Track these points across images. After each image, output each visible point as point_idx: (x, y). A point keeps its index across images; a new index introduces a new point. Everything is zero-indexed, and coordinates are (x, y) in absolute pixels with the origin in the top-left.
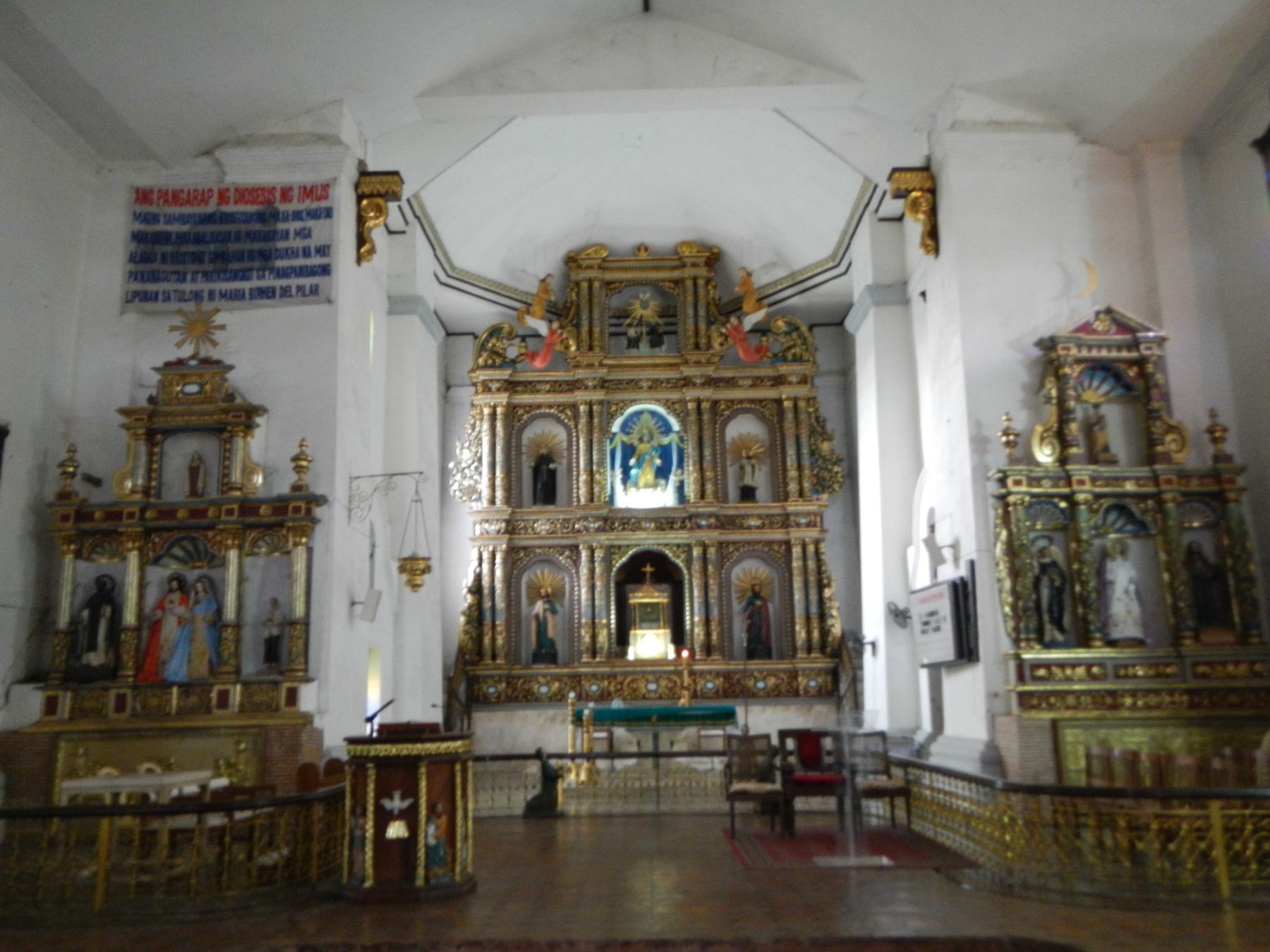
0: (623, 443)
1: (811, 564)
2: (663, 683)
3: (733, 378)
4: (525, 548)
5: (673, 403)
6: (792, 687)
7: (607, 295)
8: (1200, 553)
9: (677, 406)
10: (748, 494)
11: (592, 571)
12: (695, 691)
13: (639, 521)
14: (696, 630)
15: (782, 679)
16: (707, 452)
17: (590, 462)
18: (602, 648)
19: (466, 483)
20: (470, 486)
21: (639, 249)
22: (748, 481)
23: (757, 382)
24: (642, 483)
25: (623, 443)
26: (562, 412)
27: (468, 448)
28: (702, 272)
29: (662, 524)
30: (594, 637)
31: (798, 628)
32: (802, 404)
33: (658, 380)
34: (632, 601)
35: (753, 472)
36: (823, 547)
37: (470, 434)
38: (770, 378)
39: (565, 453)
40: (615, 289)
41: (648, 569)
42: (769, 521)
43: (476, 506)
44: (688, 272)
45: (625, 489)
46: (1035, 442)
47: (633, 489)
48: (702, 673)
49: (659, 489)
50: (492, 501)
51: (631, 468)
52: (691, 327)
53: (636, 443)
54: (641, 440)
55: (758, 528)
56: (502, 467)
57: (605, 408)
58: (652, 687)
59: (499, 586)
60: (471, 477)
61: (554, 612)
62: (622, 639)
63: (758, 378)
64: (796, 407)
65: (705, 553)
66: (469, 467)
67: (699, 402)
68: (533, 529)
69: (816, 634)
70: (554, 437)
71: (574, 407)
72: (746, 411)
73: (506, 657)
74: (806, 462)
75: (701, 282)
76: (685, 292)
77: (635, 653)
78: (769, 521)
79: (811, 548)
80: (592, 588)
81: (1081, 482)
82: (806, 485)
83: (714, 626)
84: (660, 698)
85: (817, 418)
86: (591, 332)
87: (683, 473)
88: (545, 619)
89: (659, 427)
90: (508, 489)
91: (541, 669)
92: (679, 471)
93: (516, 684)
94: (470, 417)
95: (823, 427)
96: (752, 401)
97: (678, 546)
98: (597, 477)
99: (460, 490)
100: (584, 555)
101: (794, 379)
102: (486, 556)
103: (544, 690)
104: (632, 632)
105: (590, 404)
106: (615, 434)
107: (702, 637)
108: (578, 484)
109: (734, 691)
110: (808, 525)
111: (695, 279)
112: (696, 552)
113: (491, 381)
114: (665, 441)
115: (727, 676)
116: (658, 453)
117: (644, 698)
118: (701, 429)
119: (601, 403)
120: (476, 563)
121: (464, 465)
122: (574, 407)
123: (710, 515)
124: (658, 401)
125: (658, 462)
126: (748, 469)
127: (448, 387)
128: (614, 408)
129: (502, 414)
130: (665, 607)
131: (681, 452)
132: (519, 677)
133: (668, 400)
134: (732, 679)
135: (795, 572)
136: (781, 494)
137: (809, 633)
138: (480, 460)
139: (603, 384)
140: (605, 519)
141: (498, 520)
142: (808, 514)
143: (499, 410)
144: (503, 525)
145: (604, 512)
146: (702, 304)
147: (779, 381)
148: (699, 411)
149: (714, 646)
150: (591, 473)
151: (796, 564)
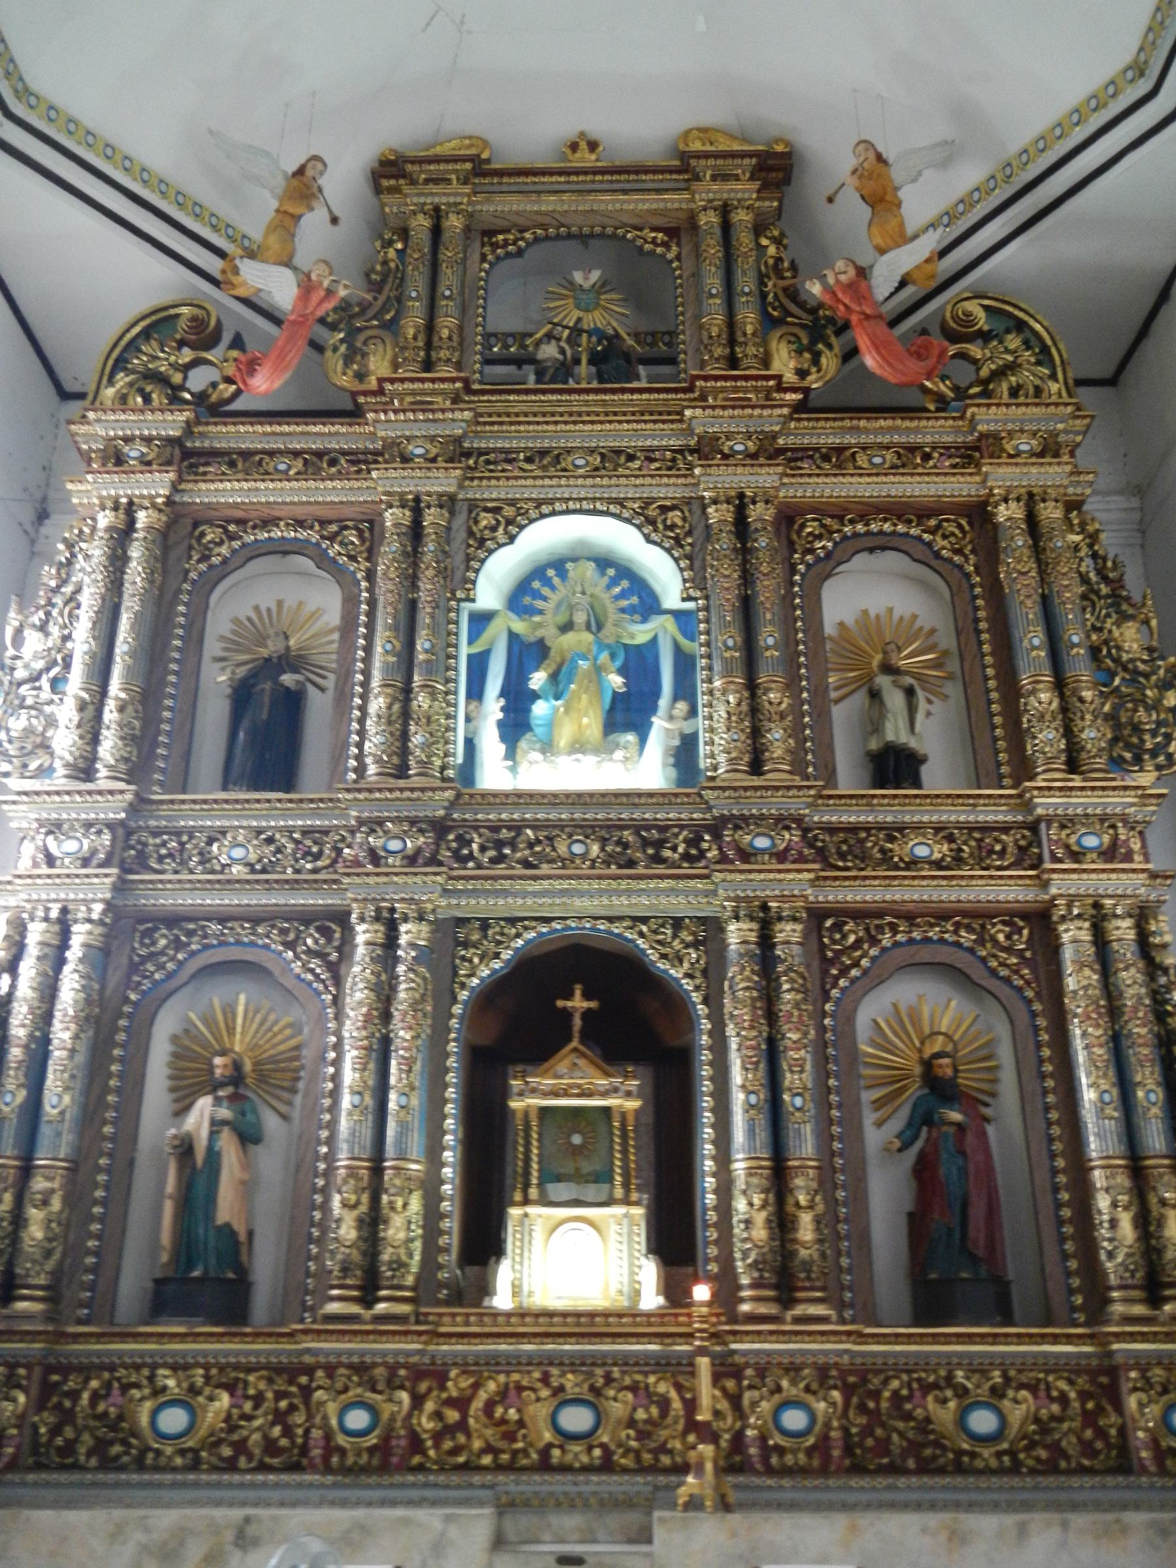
0: (513, 636)
1: (1131, 980)
2: (618, 1406)
4: (173, 920)
5: (664, 509)
6: (1101, 1433)
7: (483, 258)
9: (675, 517)
12: (738, 1438)
13: (550, 831)
14: (740, 1205)
15: (1063, 1399)
16: (768, 637)
18: (399, 1265)
21: (574, 147)
22: (895, 731)
24: (564, 738)
25: (513, 636)
26: (332, 538)
28: (744, 190)
29: (626, 846)
31: (1103, 1202)
32: (1051, 513)
33: (618, 452)
34: (515, 1104)
35: (912, 710)
36: (1163, 929)
38: (948, 450)
40: (506, 243)
41: (578, 1003)
44: (709, 191)
45: (511, 754)
47: (536, 756)
49: (619, 754)
50: (84, 770)
51: (535, 696)
52: (715, 320)
53: (549, 633)
54: (567, 627)
56: (129, 671)
57: (460, 520)
58: (577, 1419)
59: (62, 1034)
61: (249, 1137)
63: (912, 449)
64: (1032, 522)
65: (766, 941)
66: (38, 678)
67: (741, 504)
68: (205, 858)
71: (370, 528)
72: (879, 545)
73: (54, 1294)
74: (1082, 672)
75: (741, 217)
76: (697, 253)
77: (516, 1290)
79: (1123, 930)
80: (381, 1050)
83: (802, 1190)
84: (607, 1466)
87: (693, 712)
88: (213, 1156)
89: (623, 595)
92: (682, 707)
93: (75, 1395)
94: (61, 546)
96: (897, 510)
97: (677, 923)
98: (421, 701)
100: (364, 934)
101: (1025, 445)
102: (36, 933)
104: (514, 1212)
107: (760, 1233)
108: (361, 721)
109: (883, 1447)
110: (1110, 853)
111: (725, 210)
112: (738, 934)
113: (127, 440)
114: (640, 633)
116: (619, 663)
117: (545, 1465)
118: (747, 578)
119: (449, 502)
123: (782, 822)
124: (615, 508)
125: (616, 681)
126: (895, 700)
127: (42, 516)
128: (486, 520)
129: (149, 528)
130: (631, 1119)
131: (684, 664)
132: (86, 1371)
133: (647, 502)
134: (876, 1395)
135: (1076, 1006)
140: (440, 828)
141: (88, 825)
142: (1106, 820)
144: (106, 838)
145: (436, 805)
148: (741, 526)
149: (807, 1265)
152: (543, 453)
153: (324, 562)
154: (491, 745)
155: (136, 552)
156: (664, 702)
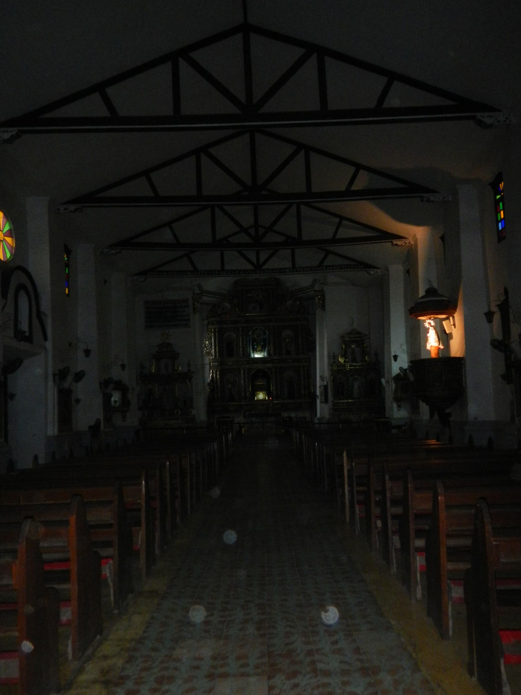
10: (288, 353)
11: (244, 375)
17: (243, 344)
19: (208, 351)
20: (209, 352)
30: (245, 394)
37: (208, 336)
43: (211, 358)
46: (340, 358)
50: (215, 356)
60: (209, 349)
62: (254, 394)
69: (307, 392)
81: (348, 366)
98: (245, 349)
103: (232, 409)
106: (250, 335)
138: (211, 344)
143: (216, 329)
150: (243, 348)
154: (251, 351)
156: (267, 345)
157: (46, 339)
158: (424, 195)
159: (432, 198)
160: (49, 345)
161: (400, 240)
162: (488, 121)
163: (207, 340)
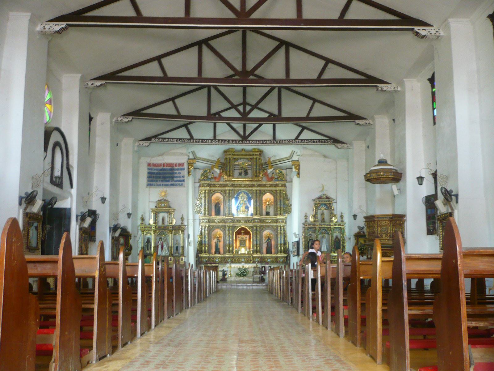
1: (282, 232)
3: (265, 185)
8: (338, 237)
10: (268, 214)
16: (258, 203)
19: (198, 209)
22: (268, 210)
23: (271, 186)
27: (199, 200)
30: (229, 248)
32: (282, 191)
39: (223, 202)
41: (243, 231)
42: (273, 221)
48: (255, 257)
50: (205, 214)
55: (270, 222)
59: (206, 235)
64: (280, 192)
69: (282, 248)
70: (220, 198)
78: (273, 221)
79: (282, 227)
81: (317, 225)
82: (282, 212)
85: (286, 195)
86: (230, 171)
90: (208, 211)
91: (217, 255)
95: (287, 197)
99: (197, 211)
100: (227, 228)
101: (280, 185)
105: (229, 190)
115: (261, 258)
118: (256, 198)
119: (232, 190)
120: (201, 230)
121: (198, 205)
122: (225, 191)
123: (258, 219)
126: (268, 207)
136: (276, 215)
137: (281, 248)
139: (233, 185)
143: (207, 191)
146: (258, 165)
147: (276, 186)
151: (279, 231)
152: (240, 184)
153: (221, 194)
155: (207, 195)
157: (72, 187)
158: (378, 85)
159: (385, 88)
160: (74, 191)
161: (362, 120)
162: (423, 33)
163: (198, 200)
